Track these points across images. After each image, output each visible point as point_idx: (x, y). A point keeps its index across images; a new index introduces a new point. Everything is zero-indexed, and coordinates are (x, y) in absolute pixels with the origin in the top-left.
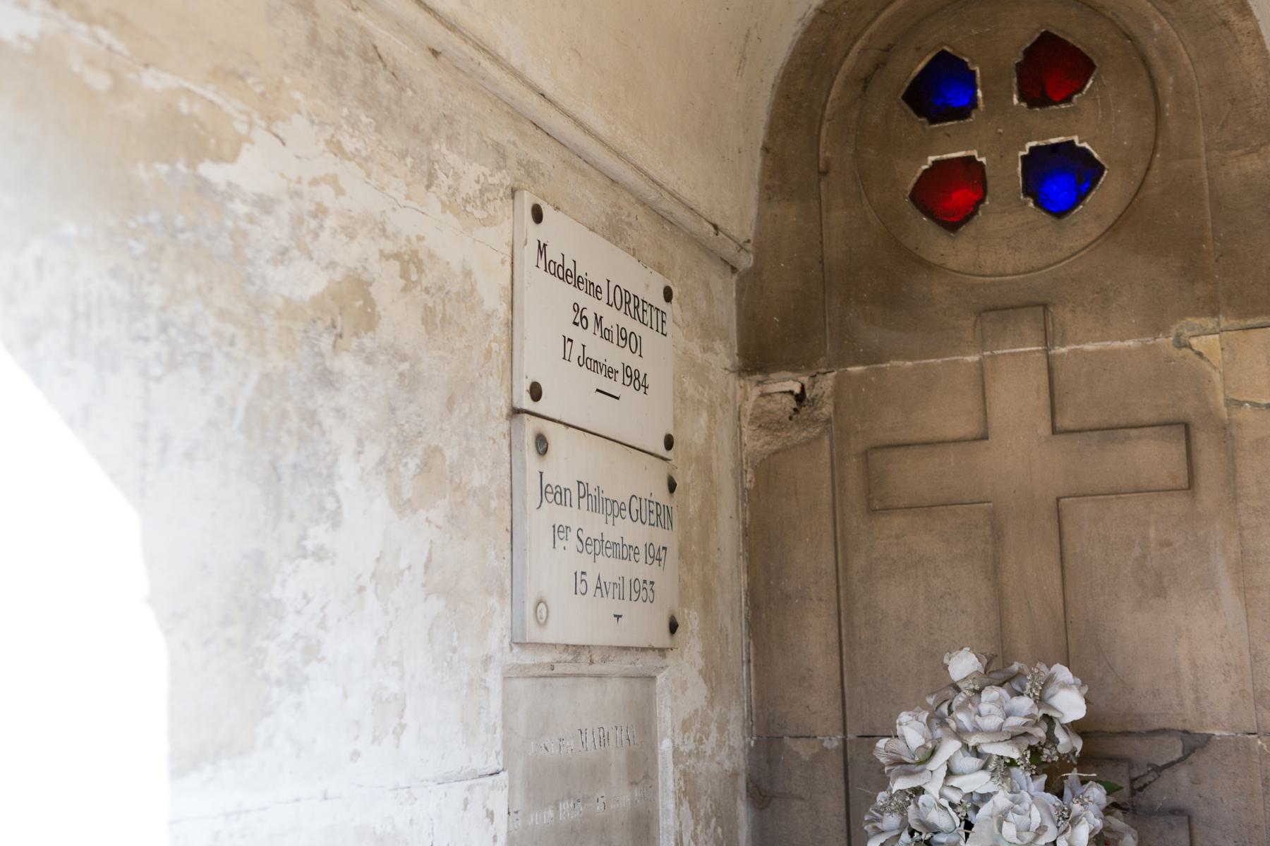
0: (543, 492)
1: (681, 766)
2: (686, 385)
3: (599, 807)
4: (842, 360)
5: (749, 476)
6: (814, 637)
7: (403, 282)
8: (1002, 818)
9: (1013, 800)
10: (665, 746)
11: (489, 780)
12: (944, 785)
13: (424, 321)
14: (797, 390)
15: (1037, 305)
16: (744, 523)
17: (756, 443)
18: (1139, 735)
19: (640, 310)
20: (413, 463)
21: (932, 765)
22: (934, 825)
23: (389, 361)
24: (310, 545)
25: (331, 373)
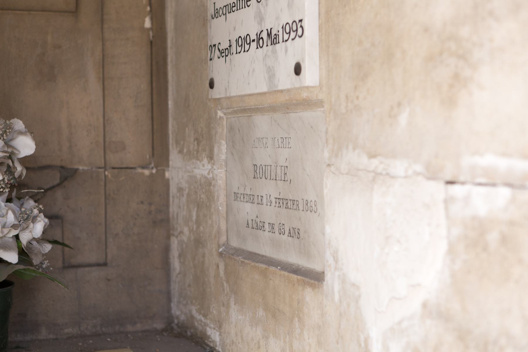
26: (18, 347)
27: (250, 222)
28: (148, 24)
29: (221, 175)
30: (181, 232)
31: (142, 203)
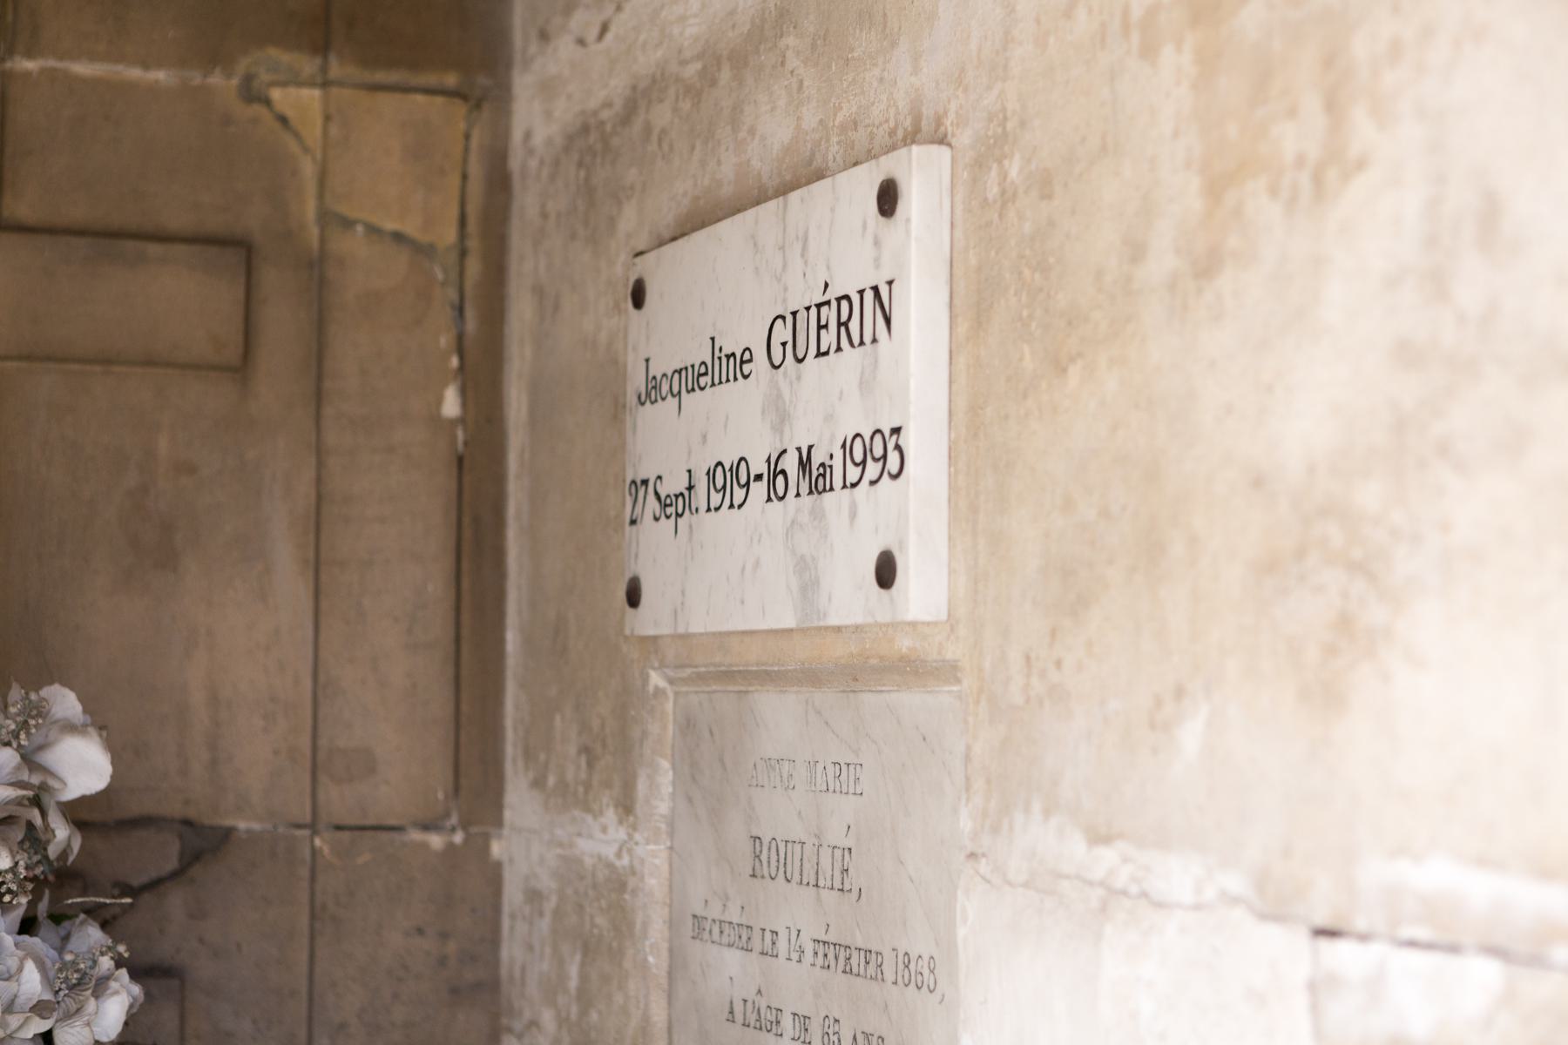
27: (738, 1008)
28: (451, 405)
29: (657, 861)
30: (534, 1023)
31: (420, 931)
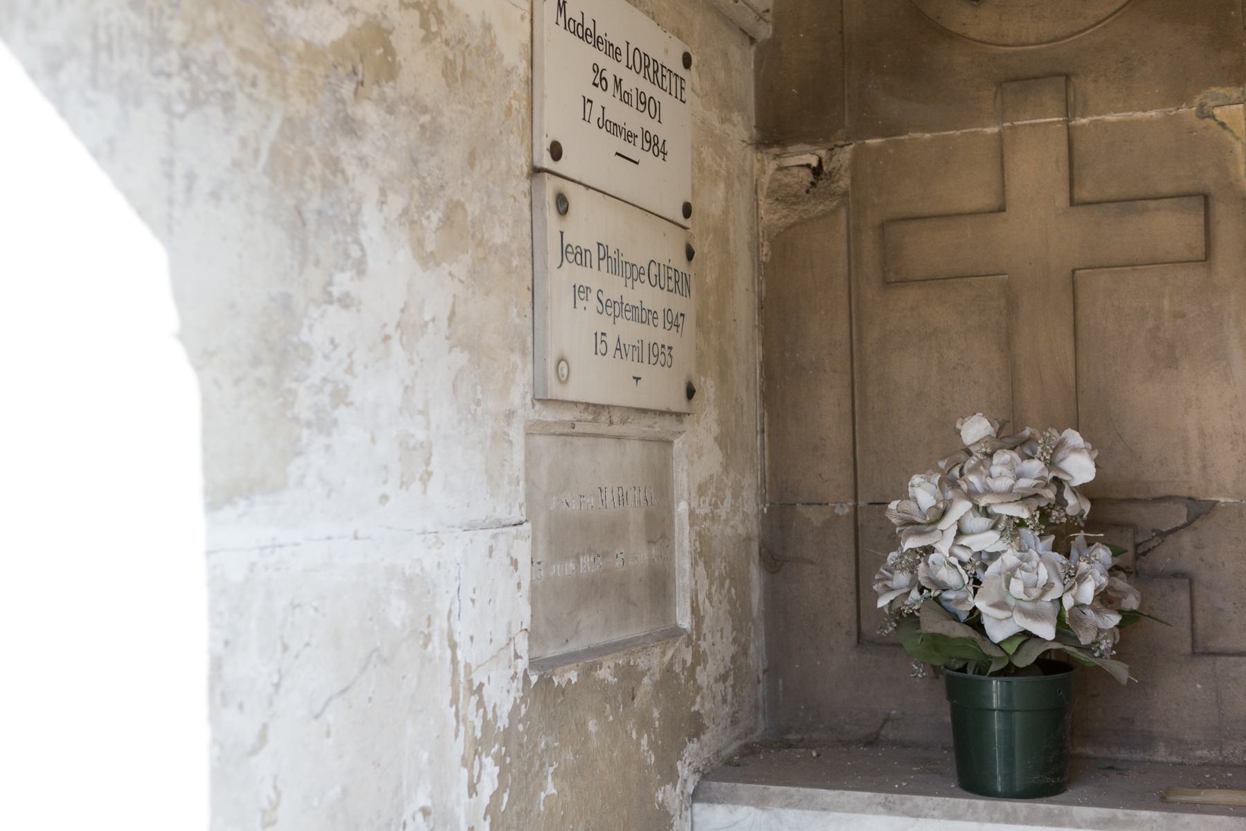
0: (564, 251)
1: (697, 528)
2: (704, 155)
3: (619, 563)
4: (860, 133)
5: (765, 250)
6: (827, 408)
7: (422, 33)
8: (1010, 574)
9: (1021, 559)
10: (682, 508)
11: (513, 529)
12: (954, 545)
13: (445, 74)
14: (814, 163)
15: (1060, 75)
16: (760, 297)
17: (772, 216)
18: (1145, 502)
19: (659, 75)
20: (435, 217)
21: (943, 525)
22: (943, 582)
23: (411, 113)
24: (336, 291)
25: (354, 120)
26: (1110, 768)
